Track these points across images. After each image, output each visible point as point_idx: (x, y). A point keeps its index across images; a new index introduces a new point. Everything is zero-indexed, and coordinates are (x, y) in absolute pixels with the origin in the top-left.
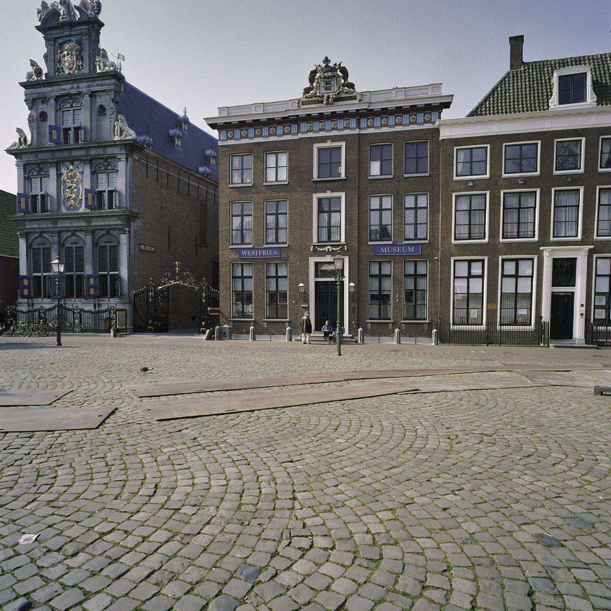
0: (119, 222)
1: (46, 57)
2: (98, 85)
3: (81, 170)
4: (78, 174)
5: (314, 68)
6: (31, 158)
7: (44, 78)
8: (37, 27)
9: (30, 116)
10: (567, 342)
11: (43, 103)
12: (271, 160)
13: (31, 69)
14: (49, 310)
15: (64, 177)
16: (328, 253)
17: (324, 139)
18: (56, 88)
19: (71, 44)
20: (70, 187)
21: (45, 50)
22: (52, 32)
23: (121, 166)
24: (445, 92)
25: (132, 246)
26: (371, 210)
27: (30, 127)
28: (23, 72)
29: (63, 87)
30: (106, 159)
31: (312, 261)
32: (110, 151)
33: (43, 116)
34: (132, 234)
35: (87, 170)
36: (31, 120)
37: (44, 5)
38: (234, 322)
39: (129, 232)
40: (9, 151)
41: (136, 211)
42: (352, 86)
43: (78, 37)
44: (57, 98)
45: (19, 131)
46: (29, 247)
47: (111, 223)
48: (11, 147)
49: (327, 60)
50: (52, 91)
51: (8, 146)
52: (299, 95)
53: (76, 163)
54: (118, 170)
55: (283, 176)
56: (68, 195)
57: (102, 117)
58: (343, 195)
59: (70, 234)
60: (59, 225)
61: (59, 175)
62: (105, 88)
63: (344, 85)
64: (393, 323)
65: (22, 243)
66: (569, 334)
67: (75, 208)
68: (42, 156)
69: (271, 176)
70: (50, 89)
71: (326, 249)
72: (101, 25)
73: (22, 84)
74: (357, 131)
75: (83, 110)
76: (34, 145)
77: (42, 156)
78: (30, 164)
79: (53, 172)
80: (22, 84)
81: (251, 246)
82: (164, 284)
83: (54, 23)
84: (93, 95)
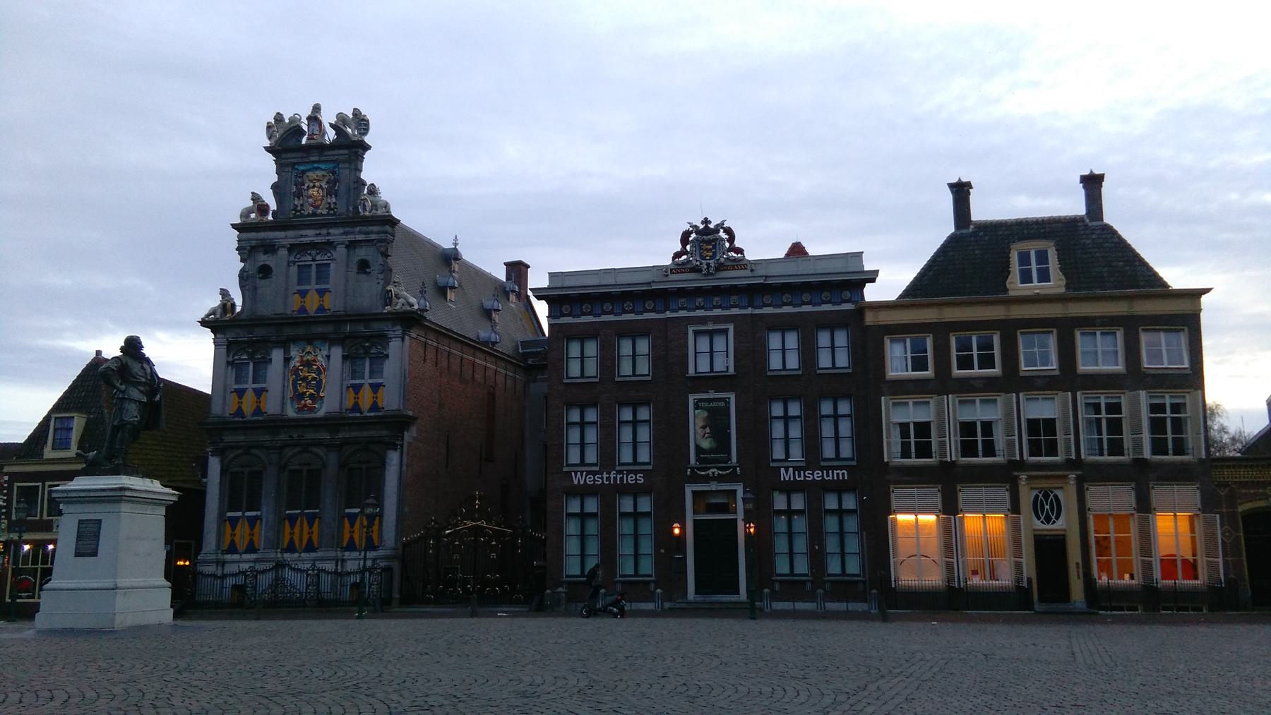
1: (275, 187)
2: (360, 233)
3: (325, 353)
4: (319, 358)
5: (687, 227)
6: (243, 336)
7: (270, 218)
8: (267, 149)
9: (242, 272)
10: (1061, 606)
11: (265, 253)
12: (626, 347)
13: (250, 203)
14: (264, 571)
15: (295, 362)
16: (714, 478)
17: (703, 320)
18: (291, 233)
19: (320, 173)
20: (304, 379)
21: (275, 178)
22: (289, 155)
23: (394, 347)
24: (868, 267)
25: (404, 468)
26: (772, 418)
27: (242, 286)
28: (236, 205)
29: (303, 232)
30: (368, 338)
31: (688, 490)
32: (376, 326)
33: (265, 271)
34: (405, 450)
35: (337, 353)
36: (244, 278)
37: (279, 118)
38: (569, 583)
39: (402, 446)
40: (204, 323)
41: (410, 413)
42: (740, 251)
43: (331, 166)
44: (292, 248)
45: (224, 293)
46: (224, 471)
47: (372, 433)
48: (208, 316)
49: (706, 221)
50: (284, 238)
51: (202, 314)
52: (668, 261)
53: (317, 343)
54: (387, 356)
55: (644, 368)
56: (300, 390)
57: (363, 276)
58: (732, 396)
61: (287, 360)
62: (373, 237)
63: (730, 249)
64: (812, 582)
65: (214, 464)
66: (1065, 595)
67: (312, 410)
68: (260, 332)
69: (626, 368)
70: (282, 234)
71: (710, 472)
72: (366, 148)
73: (234, 226)
74: (749, 311)
76: (244, 317)
77: (260, 332)
78: (237, 342)
79: (277, 355)
80: (234, 226)
81: (597, 469)
82: (456, 525)
83: (292, 143)
84: (352, 245)
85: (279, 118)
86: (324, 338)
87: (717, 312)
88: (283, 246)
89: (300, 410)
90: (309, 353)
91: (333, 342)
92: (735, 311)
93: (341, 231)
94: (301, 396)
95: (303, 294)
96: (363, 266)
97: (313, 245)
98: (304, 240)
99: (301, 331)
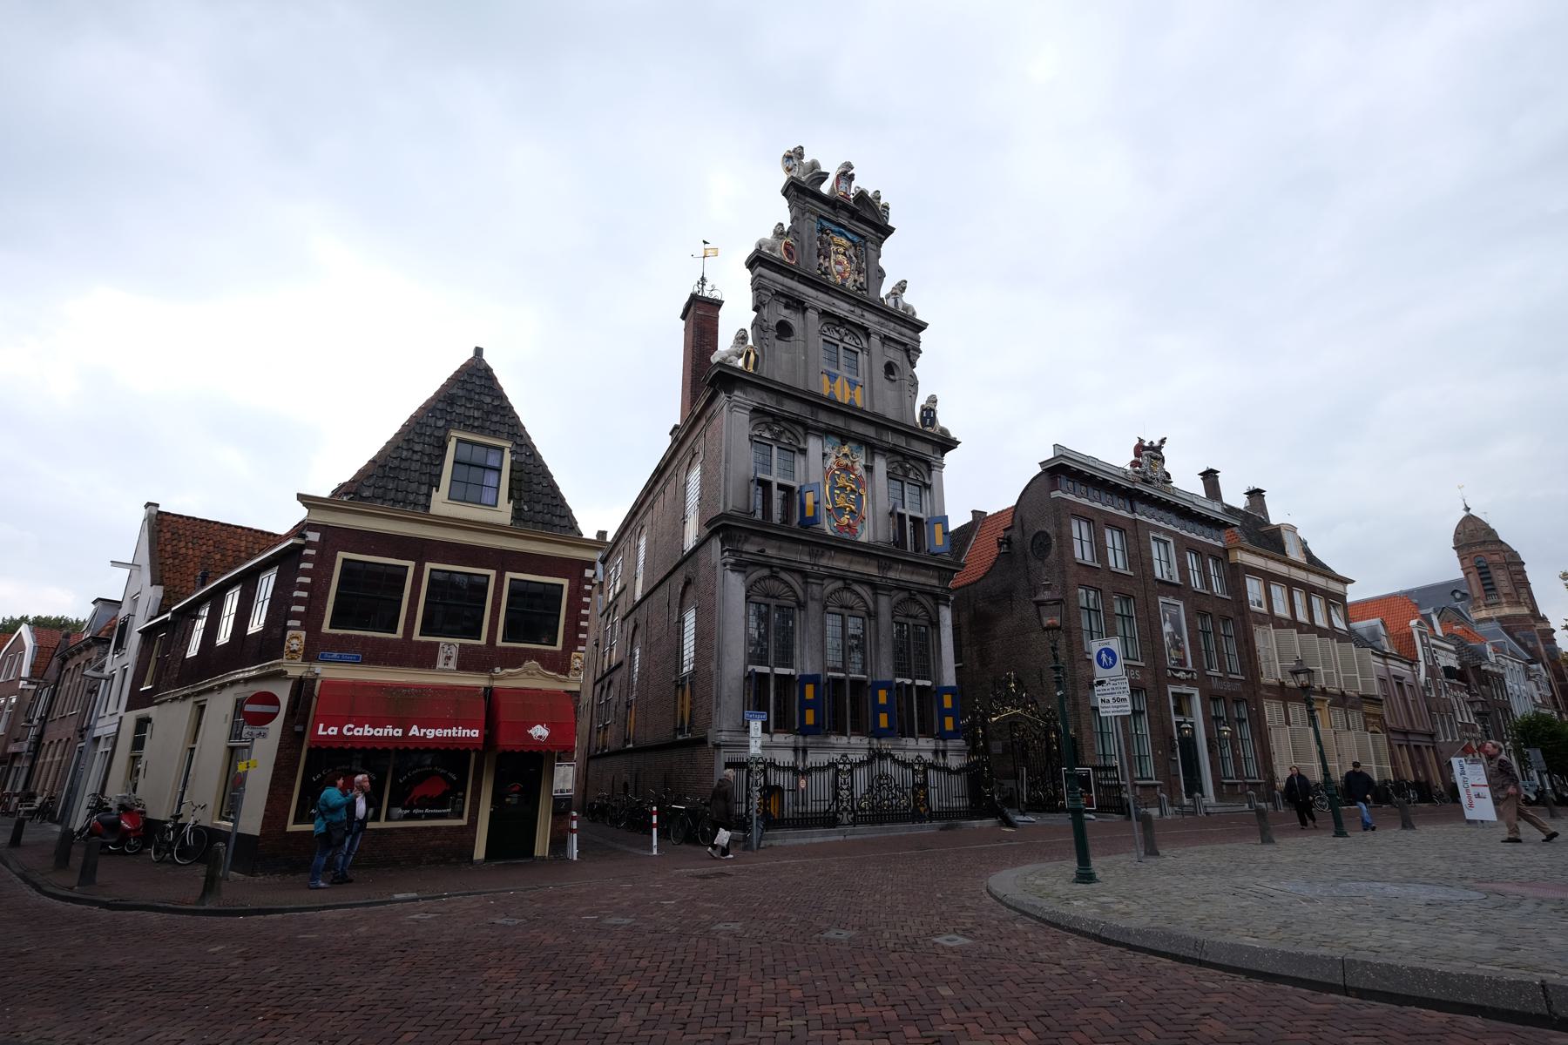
0: (935, 582)
4: (857, 466)
6: (769, 402)
11: (787, 306)
15: (831, 461)
17: (1157, 529)
18: (821, 295)
20: (843, 488)
30: (906, 457)
32: (918, 447)
33: (784, 330)
35: (881, 465)
43: (856, 239)
44: (824, 314)
47: (922, 580)
56: (841, 502)
59: (839, 584)
60: (824, 562)
61: (824, 455)
68: (790, 407)
75: (862, 358)
77: (790, 407)
84: (886, 339)
85: (798, 153)
86: (862, 441)
87: (1162, 524)
88: (815, 309)
89: (841, 528)
90: (845, 455)
91: (872, 448)
92: (1171, 527)
93: (876, 319)
94: (840, 511)
95: (833, 378)
96: (890, 368)
97: (842, 321)
98: (838, 312)
99: (839, 423)
